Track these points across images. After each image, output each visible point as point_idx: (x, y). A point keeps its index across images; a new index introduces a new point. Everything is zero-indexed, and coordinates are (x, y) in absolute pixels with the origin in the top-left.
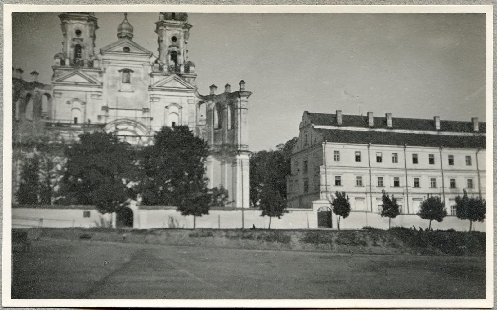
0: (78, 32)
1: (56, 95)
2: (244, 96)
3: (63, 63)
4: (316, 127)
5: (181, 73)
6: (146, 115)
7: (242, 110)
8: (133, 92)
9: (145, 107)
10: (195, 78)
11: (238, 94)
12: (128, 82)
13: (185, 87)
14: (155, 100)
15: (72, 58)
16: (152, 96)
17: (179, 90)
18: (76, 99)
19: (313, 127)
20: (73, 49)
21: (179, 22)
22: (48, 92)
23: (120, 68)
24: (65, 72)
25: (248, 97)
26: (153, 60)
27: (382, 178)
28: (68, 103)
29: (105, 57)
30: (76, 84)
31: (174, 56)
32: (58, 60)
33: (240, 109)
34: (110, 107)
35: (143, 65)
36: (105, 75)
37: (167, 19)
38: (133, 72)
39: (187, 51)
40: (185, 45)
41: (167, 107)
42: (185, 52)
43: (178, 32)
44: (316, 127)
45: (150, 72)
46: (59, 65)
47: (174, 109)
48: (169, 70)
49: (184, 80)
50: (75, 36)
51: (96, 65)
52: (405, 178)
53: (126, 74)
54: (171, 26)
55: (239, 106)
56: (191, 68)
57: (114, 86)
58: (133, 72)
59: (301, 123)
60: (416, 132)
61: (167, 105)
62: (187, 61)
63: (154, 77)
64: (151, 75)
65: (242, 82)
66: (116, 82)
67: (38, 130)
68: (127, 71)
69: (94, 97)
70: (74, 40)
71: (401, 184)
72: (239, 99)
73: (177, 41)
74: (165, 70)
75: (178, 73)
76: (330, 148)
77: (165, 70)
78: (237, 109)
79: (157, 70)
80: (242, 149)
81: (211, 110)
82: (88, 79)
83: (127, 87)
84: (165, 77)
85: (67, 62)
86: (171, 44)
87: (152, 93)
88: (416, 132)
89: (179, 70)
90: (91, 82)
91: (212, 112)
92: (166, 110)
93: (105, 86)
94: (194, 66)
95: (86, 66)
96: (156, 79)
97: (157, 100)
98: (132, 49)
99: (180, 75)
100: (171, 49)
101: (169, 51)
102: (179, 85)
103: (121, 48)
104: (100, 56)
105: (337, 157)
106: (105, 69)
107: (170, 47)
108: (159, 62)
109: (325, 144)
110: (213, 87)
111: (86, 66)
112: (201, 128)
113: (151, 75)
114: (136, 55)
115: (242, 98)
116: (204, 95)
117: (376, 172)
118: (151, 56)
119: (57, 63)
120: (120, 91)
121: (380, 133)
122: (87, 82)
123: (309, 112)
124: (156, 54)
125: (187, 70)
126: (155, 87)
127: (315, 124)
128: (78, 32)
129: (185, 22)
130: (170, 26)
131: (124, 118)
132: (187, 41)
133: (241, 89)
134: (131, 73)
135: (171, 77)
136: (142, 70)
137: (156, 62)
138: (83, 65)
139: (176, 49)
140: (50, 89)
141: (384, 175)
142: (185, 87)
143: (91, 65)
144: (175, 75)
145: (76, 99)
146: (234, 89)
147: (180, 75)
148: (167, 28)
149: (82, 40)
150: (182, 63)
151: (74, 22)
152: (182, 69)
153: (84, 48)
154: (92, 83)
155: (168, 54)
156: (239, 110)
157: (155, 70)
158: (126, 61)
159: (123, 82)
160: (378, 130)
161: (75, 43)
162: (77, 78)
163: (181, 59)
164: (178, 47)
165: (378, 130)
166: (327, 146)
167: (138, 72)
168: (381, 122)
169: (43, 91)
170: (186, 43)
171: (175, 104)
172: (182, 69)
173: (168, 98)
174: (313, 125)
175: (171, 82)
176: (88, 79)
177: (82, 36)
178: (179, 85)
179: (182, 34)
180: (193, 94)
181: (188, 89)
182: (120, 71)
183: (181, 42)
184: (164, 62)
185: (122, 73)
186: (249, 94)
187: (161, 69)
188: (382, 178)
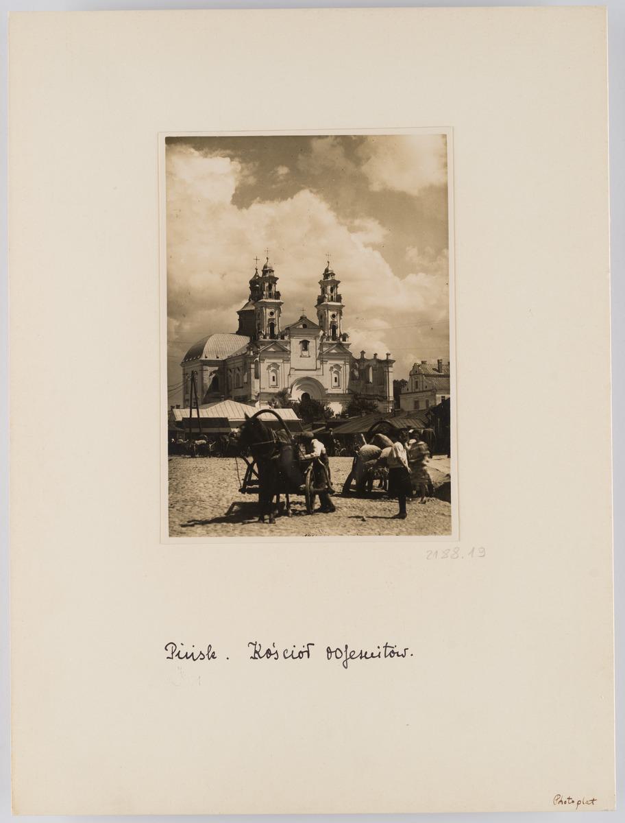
8: (309, 357)
23: (301, 340)
31: (334, 328)
56: (347, 339)
61: (332, 365)
83: (305, 353)
102: (341, 352)
103: (301, 326)
107: (331, 322)
120: (301, 356)
125: (344, 340)
133: (387, 358)
146: (382, 357)
163: (338, 332)
171: (337, 365)
177: (274, 317)
178: (341, 352)
182: (300, 342)
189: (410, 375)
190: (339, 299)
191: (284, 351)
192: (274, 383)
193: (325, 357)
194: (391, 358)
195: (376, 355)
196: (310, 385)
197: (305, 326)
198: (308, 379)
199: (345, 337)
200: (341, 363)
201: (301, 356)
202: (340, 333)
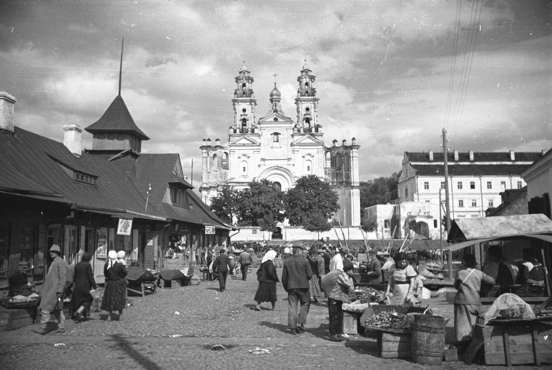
0: (244, 110)
1: (231, 153)
2: (355, 149)
3: (235, 131)
4: (412, 163)
5: (313, 133)
6: (290, 162)
7: (354, 158)
8: (281, 147)
9: (289, 157)
10: (322, 136)
11: (351, 147)
12: (278, 141)
13: (315, 142)
14: (295, 152)
15: (241, 127)
16: (293, 150)
17: (311, 145)
18: (244, 155)
19: (410, 164)
20: (241, 121)
21: (310, 97)
22: (226, 151)
23: (272, 132)
24: (236, 138)
25: (358, 149)
26: (293, 125)
27: (462, 201)
28: (239, 158)
29: (262, 125)
30: (244, 145)
32: (232, 130)
33: (353, 157)
34: (266, 159)
35: (287, 129)
36: (262, 137)
37: (301, 96)
38: (280, 134)
39: (317, 116)
40: (315, 113)
41: (303, 157)
42: (315, 117)
43: (310, 105)
44: (412, 163)
45: (292, 133)
46: (233, 133)
47: (309, 157)
48: (304, 131)
49: (315, 138)
50: (242, 113)
51: (256, 131)
52: (481, 200)
53: (275, 136)
54: (305, 100)
55: (351, 156)
56: (320, 129)
57: (268, 145)
58: (280, 134)
59: (403, 160)
60: (494, 163)
62: (316, 124)
63: (295, 137)
64: (293, 136)
65: (354, 139)
66: (270, 142)
67: (221, 177)
68: (276, 134)
69: (255, 153)
70: (241, 116)
71: (477, 205)
72: (351, 151)
73: (310, 110)
74: (302, 132)
75: (311, 133)
76: (421, 180)
77: (302, 132)
78: (350, 157)
79: (296, 132)
80: (354, 185)
81: (334, 157)
82: (251, 141)
83: (277, 144)
84: (302, 136)
85: (238, 131)
86: (305, 113)
87: (293, 148)
88: (494, 163)
89: (311, 131)
90: (254, 143)
91: (334, 159)
92: (303, 158)
93: (262, 145)
94: (321, 127)
95: (250, 132)
96: (296, 138)
97: (297, 152)
98: (279, 120)
99: (312, 135)
100: (306, 117)
101: (304, 118)
102: (311, 141)
104: (258, 126)
105: (427, 186)
106: (262, 133)
107: (305, 115)
108: (297, 126)
109: (418, 177)
110: (335, 141)
111: (250, 132)
112: (327, 170)
113: (293, 136)
114: (282, 123)
115: (354, 150)
116: (329, 147)
117: (457, 196)
118: (292, 123)
119: (232, 132)
120: (272, 147)
121: (464, 165)
122: (251, 143)
123: (409, 152)
124: (295, 120)
125: (317, 130)
126: (295, 143)
127: (412, 161)
128: (244, 110)
129: (315, 97)
130: (304, 101)
131: (275, 165)
132: (316, 110)
134: (279, 135)
135: (306, 136)
136: (286, 132)
137: (296, 126)
138: (247, 132)
139: (308, 116)
140: (228, 149)
141: (464, 198)
142: (315, 142)
143: (253, 131)
144: (308, 135)
145: (244, 155)
146: (349, 143)
147: (312, 135)
148: (303, 102)
149: (246, 115)
150: (313, 125)
151: (242, 103)
152: (313, 130)
153: (248, 120)
154: (253, 143)
155: (304, 120)
156: (351, 158)
157: (295, 132)
158: (276, 127)
159: (274, 142)
160: (461, 163)
161: (243, 117)
162: (244, 141)
164: (310, 115)
165: (461, 163)
166: (419, 179)
167: (284, 134)
168: (464, 157)
169: (223, 151)
170: (316, 111)
171: (309, 154)
172: (313, 130)
173: (303, 151)
174: (410, 162)
175: (306, 140)
176: (251, 141)
177: (246, 113)
178: (311, 141)
179: (313, 105)
180: (321, 147)
181: (318, 144)
182: (271, 134)
183: (312, 111)
184: (301, 126)
185: (273, 135)
186: (358, 147)
187: (299, 131)
188: (462, 201)
189: (403, 164)
190: (313, 92)
191: (253, 143)
192: (245, 173)
193: (295, 147)
194: (356, 143)
195: (344, 141)
196: (275, 174)
197: (276, 119)
198: (278, 168)
199: (317, 127)
200: (313, 151)
201: (272, 147)
202: (315, 124)
